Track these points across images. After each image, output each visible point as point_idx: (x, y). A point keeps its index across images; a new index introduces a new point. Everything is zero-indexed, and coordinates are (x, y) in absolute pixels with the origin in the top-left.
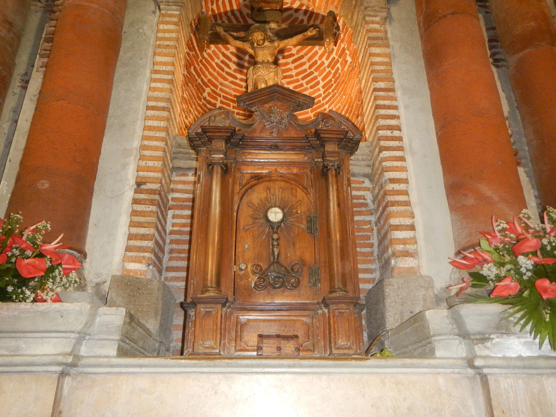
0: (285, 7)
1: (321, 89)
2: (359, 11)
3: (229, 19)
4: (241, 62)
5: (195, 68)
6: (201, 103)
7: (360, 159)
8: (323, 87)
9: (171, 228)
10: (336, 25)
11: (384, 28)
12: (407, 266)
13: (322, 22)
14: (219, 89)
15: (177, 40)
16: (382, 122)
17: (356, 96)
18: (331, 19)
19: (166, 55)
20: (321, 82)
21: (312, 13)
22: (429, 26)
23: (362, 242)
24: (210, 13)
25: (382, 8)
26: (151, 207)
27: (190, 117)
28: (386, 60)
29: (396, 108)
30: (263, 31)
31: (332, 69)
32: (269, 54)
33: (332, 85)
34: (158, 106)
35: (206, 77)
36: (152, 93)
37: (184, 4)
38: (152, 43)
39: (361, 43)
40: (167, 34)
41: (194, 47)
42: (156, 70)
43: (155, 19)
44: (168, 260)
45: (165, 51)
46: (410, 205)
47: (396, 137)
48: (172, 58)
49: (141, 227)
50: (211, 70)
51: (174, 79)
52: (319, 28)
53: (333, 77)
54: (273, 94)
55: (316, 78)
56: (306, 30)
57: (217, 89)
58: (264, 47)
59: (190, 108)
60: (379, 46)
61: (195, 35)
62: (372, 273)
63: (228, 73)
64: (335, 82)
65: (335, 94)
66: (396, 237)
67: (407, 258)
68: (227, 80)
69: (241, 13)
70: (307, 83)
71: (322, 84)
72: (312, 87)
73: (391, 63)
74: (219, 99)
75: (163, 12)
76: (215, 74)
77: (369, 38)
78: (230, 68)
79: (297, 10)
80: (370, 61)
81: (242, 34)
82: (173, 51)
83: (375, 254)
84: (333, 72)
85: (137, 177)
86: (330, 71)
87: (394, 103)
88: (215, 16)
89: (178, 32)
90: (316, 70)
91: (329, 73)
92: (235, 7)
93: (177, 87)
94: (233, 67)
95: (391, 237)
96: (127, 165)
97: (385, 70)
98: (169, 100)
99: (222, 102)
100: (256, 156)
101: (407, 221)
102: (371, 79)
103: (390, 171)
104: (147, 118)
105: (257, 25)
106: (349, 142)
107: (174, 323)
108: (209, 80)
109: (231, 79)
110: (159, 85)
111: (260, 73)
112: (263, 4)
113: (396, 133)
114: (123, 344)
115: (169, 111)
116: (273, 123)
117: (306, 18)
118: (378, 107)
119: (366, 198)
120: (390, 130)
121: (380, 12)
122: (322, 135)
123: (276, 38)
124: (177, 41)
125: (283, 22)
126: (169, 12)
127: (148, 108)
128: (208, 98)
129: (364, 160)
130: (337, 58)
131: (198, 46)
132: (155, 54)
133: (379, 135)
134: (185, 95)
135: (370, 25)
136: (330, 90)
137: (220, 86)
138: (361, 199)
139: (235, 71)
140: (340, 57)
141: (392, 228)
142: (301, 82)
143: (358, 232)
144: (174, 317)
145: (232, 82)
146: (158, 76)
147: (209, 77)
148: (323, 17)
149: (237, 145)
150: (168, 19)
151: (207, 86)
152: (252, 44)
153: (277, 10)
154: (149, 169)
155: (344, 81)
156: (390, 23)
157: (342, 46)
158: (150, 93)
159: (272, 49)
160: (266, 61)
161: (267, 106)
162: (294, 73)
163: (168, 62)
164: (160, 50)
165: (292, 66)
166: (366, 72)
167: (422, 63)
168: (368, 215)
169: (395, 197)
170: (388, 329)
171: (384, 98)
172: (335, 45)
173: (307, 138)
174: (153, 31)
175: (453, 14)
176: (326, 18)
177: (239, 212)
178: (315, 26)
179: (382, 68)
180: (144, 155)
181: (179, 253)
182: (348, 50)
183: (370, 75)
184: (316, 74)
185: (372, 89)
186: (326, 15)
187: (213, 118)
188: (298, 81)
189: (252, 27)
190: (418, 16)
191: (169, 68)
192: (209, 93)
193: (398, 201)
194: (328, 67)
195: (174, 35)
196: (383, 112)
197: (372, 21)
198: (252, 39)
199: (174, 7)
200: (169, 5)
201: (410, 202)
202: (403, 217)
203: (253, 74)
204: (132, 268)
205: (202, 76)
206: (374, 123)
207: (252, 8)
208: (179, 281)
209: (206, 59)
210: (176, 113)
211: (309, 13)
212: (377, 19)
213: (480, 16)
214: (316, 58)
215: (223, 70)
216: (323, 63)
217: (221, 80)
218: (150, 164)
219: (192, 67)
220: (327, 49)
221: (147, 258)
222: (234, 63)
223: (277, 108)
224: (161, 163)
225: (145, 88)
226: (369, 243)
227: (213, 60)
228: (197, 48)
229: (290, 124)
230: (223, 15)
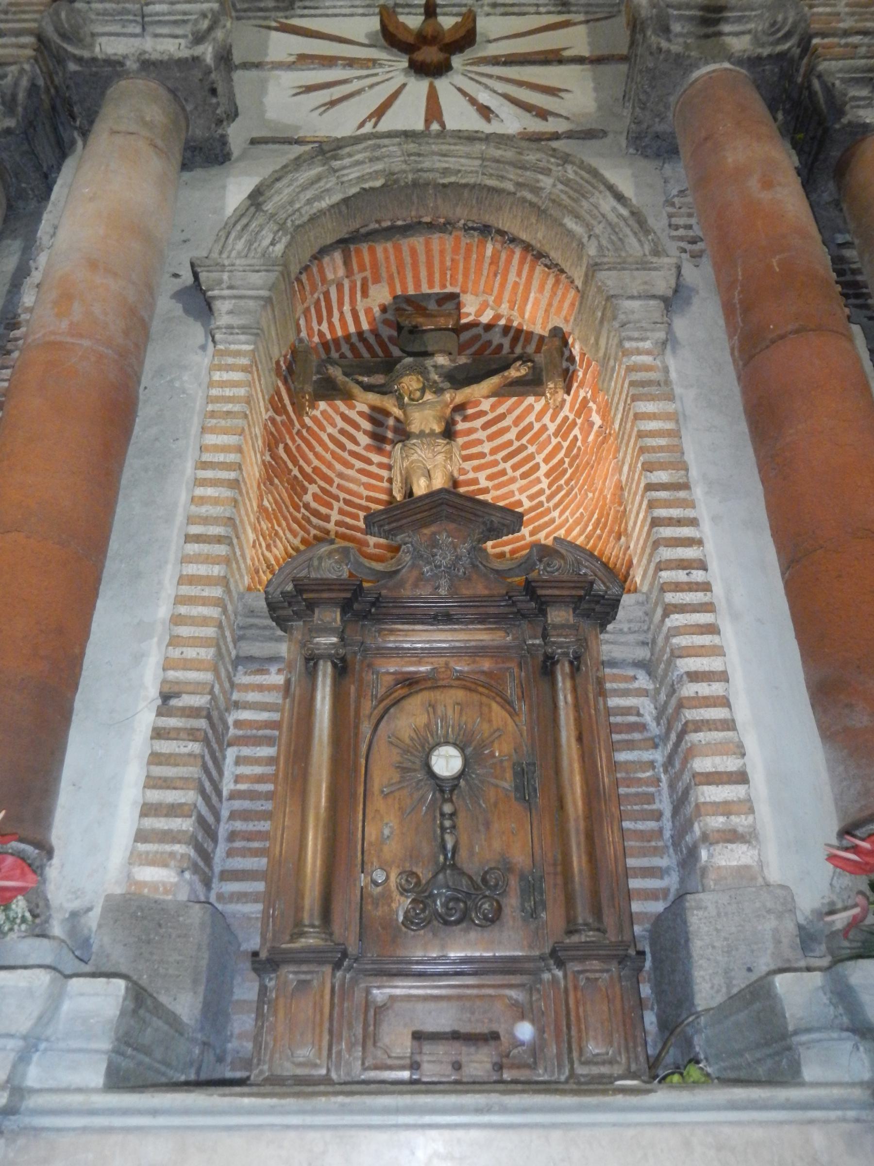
0: (464, 321)
1: (543, 479)
2: (609, 331)
3: (353, 348)
4: (379, 430)
5: (287, 449)
6: (299, 516)
7: (626, 630)
8: (547, 475)
9: (232, 786)
10: (567, 354)
11: (663, 362)
12: (735, 863)
13: (538, 350)
14: (335, 485)
15: (248, 400)
16: (667, 553)
17: (614, 495)
18: (557, 342)
19: (225, 432)
20: (542, 465)
21: (519, 331)
22: (751, 357)
23: (636, 807)
24: (316, 339)
25: (655, 323)
26: (191, 744)
27: (275, 546)
28: (669, 425)
29: (693, 522)
30: (421, 373)
31: (564, 438)
32: (434, 417)
33: (565, 471)
34: (209, 533)
35: (308, 462)
36: (197, 509)
37: (262, 330)
38: (198, 408)
39: (617, 391)
40: (227, 390)
41: (284, 406)
42: (205, 462)
43: (204, 360)
44: (224, 855)
45: (223, 423)
46: (734, 729)
47: (697, 583)
48: (236, 437)
49: (168, 788)
50: (319, 449)
51: (241, 479)
52: (532, 361)
53: (567, 455)
54: (439, 509)
55: (531, 457)
56: (507, 367)
57: (331, 486)
58: (424, 403)
59: (276, 527)
60: (652, 398)
61: (285, 382)
62: (662, 878)
63: (353, 454)
64: (571, 465)
65: (572, 489)
66: (708, 800)
67: (734, 846)
68: (351, 467)
69: (377, 336)
70: (515, 468)
71: (544, 468)
72: (524, 476)
73: (679, 431)
74: (336, 505)
75: (221, 347)
76: (328, 456)
77: (632, 384)
78: (357, 443)
79: (489, 327)
80: (636, 429)
81: (379, 379)
82: (240, 422)
83: (667, 834)
84: (565, 444)
85: (164, 681)
86: (559, 443)
87: (689, 513)
88: (325, 345)
89: (249, 384)
90: (531, 441)
91: (558, 447)
92: (365, 326)
93: (248, 493)
94: (364, 440)
95: (697, 799)
96: (143, 655)
97: (668, 446)
98: (230, 521)
99: (341, 512)
100: (406, 636)
101: (731, 764)
102: (639, 465)
103: (689, 656)
104: (186, 559)
105: (409, 360)
106: (598, 602)
107: (235, 997)
108: (316, 470)
109: (359, 464)
110: (210, 492)
111: (415, 457)
112: (421, 320)
113: (698, 576)
114: (120, 1059)
115: (231, 544)
116: (440, 567)
117: (506, 342)
118: (656, 522)
119: (641, 711)
120: (684, 569)
121: (653, 330)
122: (540, 592)
123: (447, 385)
124: (248, 403)
125: (462, 349)
126: (233, 347)
127: (189, 538)
128: (314, 505)
129: (635, 632)
130: (571, 417)
131: (293, 404)
132: (204, 430)
133: (661, 581)
134: (266, 503)
135: (633, 358)
136: (562, 482)
137: (337, 481)
138: (631, 715)
139: (368, 448)
140: (578, 414)
141: (697, 780)
142: (502, 466)
143: (628, 787)
144: (235, 982)
145: (361, 471)
146: (209, 474)
147: (316, 463)
148: (542, 338)
149: (365, 616)
150: (230, 360)
151: (312, 481)
152: (400, 398)
153: (447, 329)
154: (187, 665)
155: (588, 463)
156: (674, 351)
157: (582, 394)
158: (193, 508)
159: (439, 408)
160: (427, 431)
161: (426, 531)
162: (486, 448)
163: (229, 446)
164: (214, 421)
165: (482, 435)
166: (630, 451)
167: (743, 427)
168: (647, 750)
169: (702, 711)
170: (699, 1009)
171: (668, 504)
172: (568, 393)
173: (510, 598)
174: (200, 385)
175: (797, 332)
176: (546, 340)
177: (370, 755)
178: (524, 358)
179: (662, 442)
180: (178, 636)
181: (248, 840)
182: (595, 402)
183: (638, 457)
184: (531, 449)
185: (642, 485)
186: (546, 334)
187: (316, 563)
188: (495, 463)
189: (398, 366)
190: (731, 337)
191: (232, 457)
192: (315, 496)
193: (708, 721)
194: (556, 434)
195: (242, 392)
196: (667, 532)
197: (637, 349)
198: (398, 389)
199: (243, 338)
200: (232, 334)
201: (733, 721)
202: (721, 754)
203: (403, 458)
204: (148, 878)
205: (302, 462)
206: (651, 555)
207: (399, 328)
208: (246, 902)
209: (309, 429)
210: (245, 546)
211: (511, 334)
212: (647, 345)
213: (856, 329)
214: (531, 418)
215: (343, 447)
216: (544, 428)
217: (338, 467)
218: (191, 653)
219: (281, 446)
220: (551, 401)
221: (179, 857)
222: (365, 432)
223: (448, 536)
224: (212, 651)
225: (183, 498)
226: (652, 811)
227: (323, 429)
228: (290, 408)
229: (474, 566)
230: (342, 342)
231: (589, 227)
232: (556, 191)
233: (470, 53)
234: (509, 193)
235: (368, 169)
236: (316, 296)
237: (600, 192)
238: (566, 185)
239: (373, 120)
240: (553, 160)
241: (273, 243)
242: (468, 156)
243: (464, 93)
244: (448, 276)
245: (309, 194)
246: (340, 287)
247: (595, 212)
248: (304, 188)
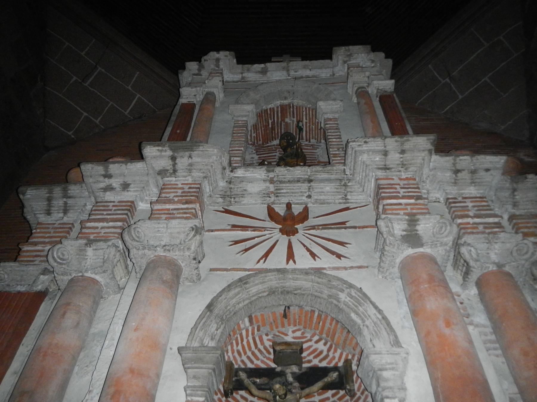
199: (199, 393)
231: (363, 321)
232: (346, 300)
233: (306, 223)
234: (325, 299)
235: (260, 287)
236: (236, 336)
237: (367, 304)
238: (351, 298)
239: (264, 259)
240: (345, 286)
241: (217, 330)
242: (306, 280)
243: (304, 246)
244: (297, 322)
245: (234, 301)
246: (247, 331)
247: (365, 313)
248: (232, 298)
